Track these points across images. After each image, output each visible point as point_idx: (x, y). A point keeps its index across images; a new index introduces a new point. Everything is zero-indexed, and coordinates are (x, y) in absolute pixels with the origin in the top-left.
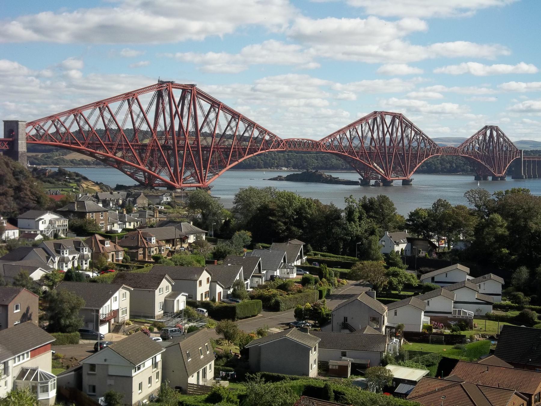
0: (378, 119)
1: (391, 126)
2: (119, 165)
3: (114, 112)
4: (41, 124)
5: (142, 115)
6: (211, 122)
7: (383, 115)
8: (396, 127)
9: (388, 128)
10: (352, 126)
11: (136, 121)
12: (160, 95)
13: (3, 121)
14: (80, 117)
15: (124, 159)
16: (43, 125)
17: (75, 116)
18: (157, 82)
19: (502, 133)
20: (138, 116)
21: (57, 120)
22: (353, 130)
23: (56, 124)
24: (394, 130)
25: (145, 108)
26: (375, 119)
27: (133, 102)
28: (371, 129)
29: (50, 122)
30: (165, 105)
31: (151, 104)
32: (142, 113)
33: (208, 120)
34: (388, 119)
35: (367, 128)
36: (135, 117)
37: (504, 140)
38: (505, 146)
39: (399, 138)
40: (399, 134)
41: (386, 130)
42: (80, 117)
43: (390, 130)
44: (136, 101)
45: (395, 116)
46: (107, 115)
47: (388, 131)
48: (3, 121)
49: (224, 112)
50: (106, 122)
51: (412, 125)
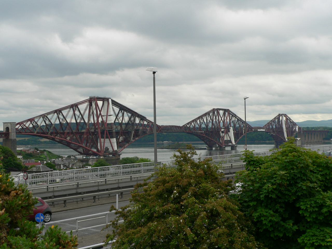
0: (216, 112)
1: (223, 117)
2: (68, 145)
3: (65, 115)
4: (24, 124)
5: (80, 116)
6: (119, 118)
7: (218, 110)
8: (226, 117)
9: (221, 118)
10: (201, 117)
11: (78, 120)
12: (91, 105)
13: (3, 123)
14: (46, 119)
15: (70, 141)
16: (25, 124)
17: (43, 118)
18: (89, 98)
19: (289, 118)
20: (79, 117)
21: (33, 121)
22: (201, 119)
23: (33, 123)
24: (225, 119)
25: (82, 112)
26: (214, 113)
27: (75, 110)
28: (212, 118)
29: (29, 122)
30: (93, 110)
31: (86, 110)
32: (80, 115)
33: (118, 117)
34: (221, 112)
35: (209, 119)
36: (77, 117)
37: (291, 122)
38: (291, 125)
39: (228, 123)
40: (228, 121)
41: (220, 119)
42: (46, 119)
43: (223, 119)
44: (77, 108)
45: (225, 111)
46: (61, 116)
47: (221, 119)
48: (3, 123)
49: (127, 112)
50: (61, 121)
51: (235, 115)
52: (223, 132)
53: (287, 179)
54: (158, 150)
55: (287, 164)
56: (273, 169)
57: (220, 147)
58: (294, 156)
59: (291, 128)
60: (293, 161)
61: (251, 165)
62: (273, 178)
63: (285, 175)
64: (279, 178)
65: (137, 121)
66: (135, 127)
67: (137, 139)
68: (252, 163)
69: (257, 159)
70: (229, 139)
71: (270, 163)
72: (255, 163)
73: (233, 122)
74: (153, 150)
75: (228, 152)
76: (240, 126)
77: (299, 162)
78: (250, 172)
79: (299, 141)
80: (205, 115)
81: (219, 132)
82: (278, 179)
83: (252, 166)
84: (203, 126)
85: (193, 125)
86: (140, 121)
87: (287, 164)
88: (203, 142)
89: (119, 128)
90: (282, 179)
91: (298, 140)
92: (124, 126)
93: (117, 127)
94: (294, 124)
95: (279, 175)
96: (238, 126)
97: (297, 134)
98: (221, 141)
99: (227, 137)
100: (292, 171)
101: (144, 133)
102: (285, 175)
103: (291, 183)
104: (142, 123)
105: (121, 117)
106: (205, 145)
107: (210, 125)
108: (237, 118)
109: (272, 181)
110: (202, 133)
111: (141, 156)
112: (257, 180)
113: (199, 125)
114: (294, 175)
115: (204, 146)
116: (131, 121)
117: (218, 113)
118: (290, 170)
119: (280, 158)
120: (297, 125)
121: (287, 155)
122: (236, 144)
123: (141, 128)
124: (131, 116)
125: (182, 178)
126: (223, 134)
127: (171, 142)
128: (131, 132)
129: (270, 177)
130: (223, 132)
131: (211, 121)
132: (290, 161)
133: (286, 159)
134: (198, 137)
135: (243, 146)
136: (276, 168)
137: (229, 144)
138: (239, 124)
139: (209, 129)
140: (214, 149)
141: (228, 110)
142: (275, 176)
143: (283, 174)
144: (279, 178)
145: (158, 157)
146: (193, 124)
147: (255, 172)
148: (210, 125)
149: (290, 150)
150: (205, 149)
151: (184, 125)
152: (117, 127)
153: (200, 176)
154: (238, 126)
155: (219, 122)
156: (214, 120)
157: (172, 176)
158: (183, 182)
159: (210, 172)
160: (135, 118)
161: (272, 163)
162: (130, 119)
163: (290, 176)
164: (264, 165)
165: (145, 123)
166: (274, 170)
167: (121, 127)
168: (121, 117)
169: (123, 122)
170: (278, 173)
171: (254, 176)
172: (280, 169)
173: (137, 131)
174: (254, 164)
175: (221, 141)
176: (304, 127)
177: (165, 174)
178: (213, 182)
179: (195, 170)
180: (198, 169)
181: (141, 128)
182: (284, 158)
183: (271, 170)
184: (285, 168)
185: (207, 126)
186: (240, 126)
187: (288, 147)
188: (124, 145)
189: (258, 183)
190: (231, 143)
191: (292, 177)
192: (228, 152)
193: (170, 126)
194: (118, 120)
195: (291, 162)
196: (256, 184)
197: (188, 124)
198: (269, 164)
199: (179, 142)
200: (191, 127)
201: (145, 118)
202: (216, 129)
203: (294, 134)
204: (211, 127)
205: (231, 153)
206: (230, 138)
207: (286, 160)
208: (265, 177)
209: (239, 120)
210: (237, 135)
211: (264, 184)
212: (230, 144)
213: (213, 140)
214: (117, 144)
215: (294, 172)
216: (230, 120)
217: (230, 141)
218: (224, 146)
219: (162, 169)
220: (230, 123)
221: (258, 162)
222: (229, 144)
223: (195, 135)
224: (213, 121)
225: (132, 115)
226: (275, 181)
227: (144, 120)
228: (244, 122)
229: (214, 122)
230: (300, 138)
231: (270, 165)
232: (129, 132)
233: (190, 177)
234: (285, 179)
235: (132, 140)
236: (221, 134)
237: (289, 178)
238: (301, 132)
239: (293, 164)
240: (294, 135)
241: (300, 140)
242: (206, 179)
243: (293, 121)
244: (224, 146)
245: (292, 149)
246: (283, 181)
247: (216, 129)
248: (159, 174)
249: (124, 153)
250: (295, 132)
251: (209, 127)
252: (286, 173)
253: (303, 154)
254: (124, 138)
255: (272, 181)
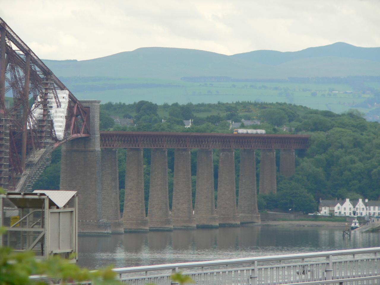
38: (14, 85)
59: (8, 106)
79: (64, 219)
91: (52, 204)
94: (33, 74)
97: (56, 156)
120: (63, 88)
176: (115, 101)
203: (37, 156)
230: (71, 194)
238: (86, 140)
240: (30, 165)
241: (70, 203)
243: (28, 52)
250: (39, 146)
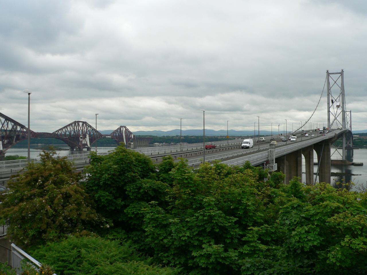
0: (77, 124)
1: (82, 127)
6: (5, 126)
7: (78, 122)
9: (81, 128)
10: (66, 127)
26: (75, 124)
28: (74, 128)
33: (4, 126)
34: (81, 124)
35: (72, 128)
39: (86, 131)
40: (85, 130)
45: (84, 123)
47: (81, 129)
51: (91, 126)
52: (81, 138)
53: (119, 171)
54: (31, 150)
55: (119, 161)
56: (109, 164)
57: (79, 148)
58: (124, 155)
60: (123, 158)
61: (95, 161)
62: (109, 170)
63: (117, 168)
64: (113, 170)
65: (19, 128)
66: (17, 133)
67: (18, 142)
68: (96, 160)
69: (99, 157)
70: (86, 143)
71: (108, 160)
72: (98, 160)
73: (89, 131)
74: (27, 150)
75: (85, 152)
76: (94, 134)
77: (126, 159)
78: (94, 166)
80: (69, 125)
81: (79, 138)
82: (112, 171)
83: (95, 162)
84: (68, 133)
85: (60, 133)
86: (21, 129)
87: (119, 161)
88: (67, 145)
89: (4, 133)
90: (115, 171)
92: (8, 133)
93: (2, 133)
95: (113, 168)
96: (92, 133)
98: (80, 144)
99: (84, 141)
100: (122, 166)
101: (24, 137)
102: (117, 168)
103: (121, 173)
104: (22, 130)
105: (6, 125)
106: (68, 147)
107: (73, 133)
108: (92, 128)
109: (109, 172)
110: (66, 138)
111: (20, 155)
112: (98, 172)
113: (64, 132)
114: (123, 168)
115: (68, 148)
116: (14, 129)
117: (79, 124)
118: (120, 164)
119: (114, 156)
121: (119, 155)
122: (91, 146)
123: (21, 134)
124: (14, 125)
125: (45, 171)
126: (82, 139)
127: (43, 144)
128: (13, 137)
129: (107, 169)
130: (81, 138)
131: (73, 129)
132: (121, 159)
133: (118, 157)
134: (63, 141)
135: (94, 148)
136: (111, 163)
137: (86, 146)
138: (93, 132)
139: (71, 136)
140: (75, 150)
141: (86, 122)
142: (111, 169)
143: (116, 168)
144: (113, 170)
145: (30, 155)
146: (60, 131)
147: (97, 166)
148: (73, 133)
149: (121, 151)
150: (69, 150)
151: (53, 133)
152: (2, 133)
153: (58, 169)
154: (92, 133)
155: (79, 131)
156: (76, 129)
157: (38, 169)
158: (45, 173)
159: (65, 167)
160: (17, 126)
161: (109, 160)
162: (13, 127)
163: (120, 169)
164: (103, 161)
165: (25, 130)
166: (110, 165)
167: (6, 133)
168: (6, 125)
169: (8, 129)
170: (112, 167)
171: (96, 169)
172: (114, 164)
173: (18, 136)
174: (97, 160)
175: (80, 144)
177: (33, 168)
178: (68, 174)
179: (55, 165)
180: (57, 164)
181: (21, 134)
182: (117, 156)
183: (108, 165)
184: (117, 163)
185: (70, 133)
186: (94, 134)
187: (120, 149)
188: (8, 146)
189: (99, 174)
190: (88, 146)
191: (122, 169)
192: (85, 152)
193: (43, 133)
194: (4, 127)
195: (121, 159)
196: (97, 174)
197: (56, 131)
198: (107, 161)
199: (50, 145)
200: (59, 134)
201: (24, 126)
202: (77, 136)
204: (73, 134)
205: (86, 152)
206: (86, 142)
207: (118, 158)
208: (104, 170)
209: (93, 129)
210: (91, 140)
211: (103, 174)
212: (87, 146)
213: (74, 143)
214: (3, 146)
215: (123, 166)
216: (87, 129)
217: (87, 144)
218: (82, 148)
219: (31, 164)
220: (87, 132)
221: (100, 160)
222: (86, 146)
223: (61, 139)
224: (74, 129)
225: (15, 124)
226: (110, 172)
227: (24, 128)
228: (97, 131)
229: (75, 131)
231: (108, 162)
232: (12, 137)
233: (51, 169)
234: (116, 171)
235: (14, 143)
236: (81, 140)
237: (119, 170)
239: (123, 160)
242: (62, 171)
244: (82, 148)
245: (122, 150)
246: (116, 172)
247: (77, 136)
248: (28, 168)
249: (7, 152)
251: (71, 134)
252: (117, 167)
253: (130, 154)
254: (8, 141)
255: (109, 172)
